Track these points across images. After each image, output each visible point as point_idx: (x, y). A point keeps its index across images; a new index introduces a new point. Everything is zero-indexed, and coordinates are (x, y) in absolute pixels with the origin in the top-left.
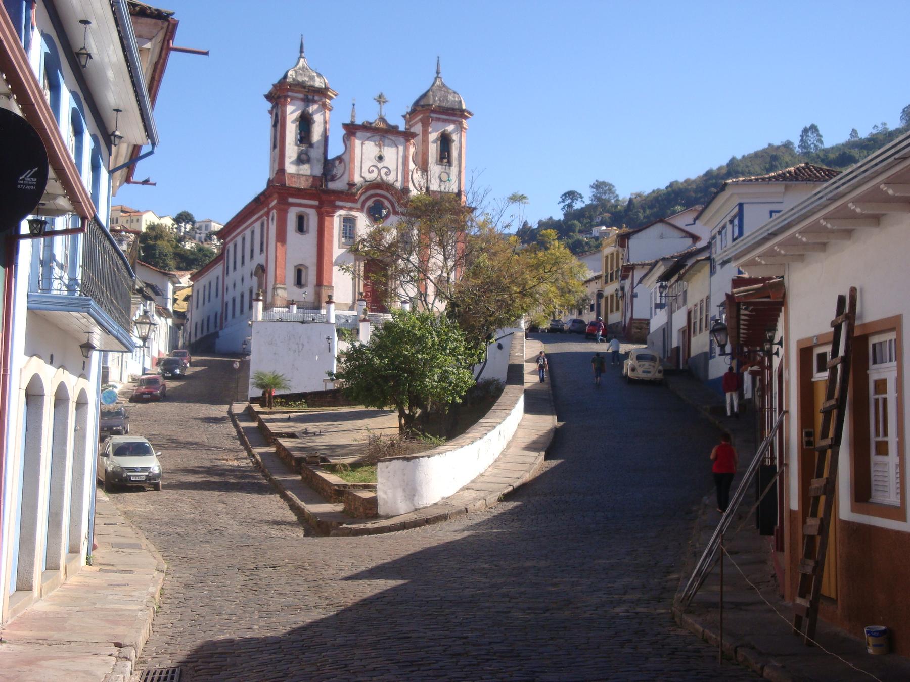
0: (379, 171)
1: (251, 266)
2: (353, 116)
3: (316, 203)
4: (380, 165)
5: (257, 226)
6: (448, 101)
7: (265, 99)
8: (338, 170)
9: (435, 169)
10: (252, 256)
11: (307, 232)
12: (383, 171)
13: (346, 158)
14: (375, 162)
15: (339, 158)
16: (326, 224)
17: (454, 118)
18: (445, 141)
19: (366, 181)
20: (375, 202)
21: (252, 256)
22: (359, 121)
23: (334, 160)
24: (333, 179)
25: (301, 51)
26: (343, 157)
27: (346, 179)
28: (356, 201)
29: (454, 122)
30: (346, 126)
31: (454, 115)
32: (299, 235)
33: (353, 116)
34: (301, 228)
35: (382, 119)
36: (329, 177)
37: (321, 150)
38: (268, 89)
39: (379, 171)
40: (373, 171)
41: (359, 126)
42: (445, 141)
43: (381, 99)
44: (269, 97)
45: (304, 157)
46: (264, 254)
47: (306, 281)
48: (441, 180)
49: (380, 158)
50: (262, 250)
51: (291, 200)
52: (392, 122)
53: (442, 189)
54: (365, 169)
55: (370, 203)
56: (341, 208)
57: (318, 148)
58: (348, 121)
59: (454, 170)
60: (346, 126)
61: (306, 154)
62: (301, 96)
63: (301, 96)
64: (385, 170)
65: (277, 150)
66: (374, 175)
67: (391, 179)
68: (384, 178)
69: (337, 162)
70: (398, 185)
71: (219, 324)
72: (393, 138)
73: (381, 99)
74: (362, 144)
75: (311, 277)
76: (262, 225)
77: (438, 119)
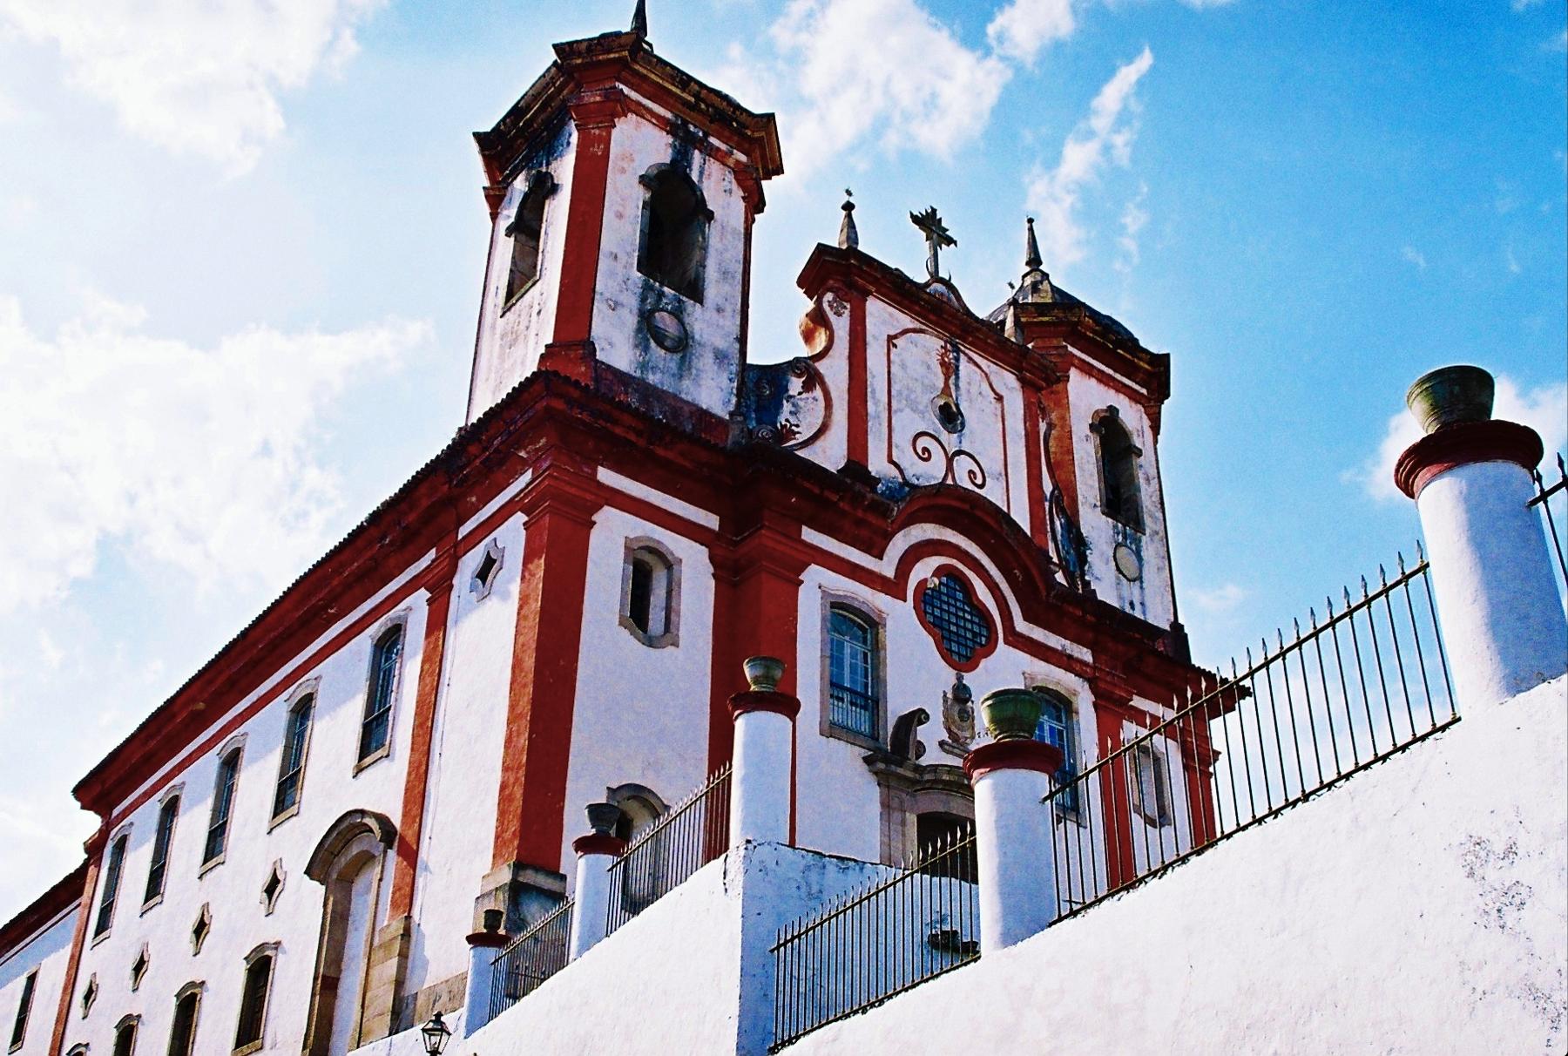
0: (950, 468)
3: (711, 521)
4: (951, 441)
7: (474, 147)
8: (803, 413)
12: (962, 466)
13: (835, 371)
14: (933, 424)
19: (906, 483)
20: (938, 572)
26: (821, 366)
29: (1133, 396)
32: (628, 641)
39: (950, 468)
40: (925, 450)
45: (665, 321)
54: (902, 439)
61: (678, 313)
66: (931, 472)
69: (796, 384)
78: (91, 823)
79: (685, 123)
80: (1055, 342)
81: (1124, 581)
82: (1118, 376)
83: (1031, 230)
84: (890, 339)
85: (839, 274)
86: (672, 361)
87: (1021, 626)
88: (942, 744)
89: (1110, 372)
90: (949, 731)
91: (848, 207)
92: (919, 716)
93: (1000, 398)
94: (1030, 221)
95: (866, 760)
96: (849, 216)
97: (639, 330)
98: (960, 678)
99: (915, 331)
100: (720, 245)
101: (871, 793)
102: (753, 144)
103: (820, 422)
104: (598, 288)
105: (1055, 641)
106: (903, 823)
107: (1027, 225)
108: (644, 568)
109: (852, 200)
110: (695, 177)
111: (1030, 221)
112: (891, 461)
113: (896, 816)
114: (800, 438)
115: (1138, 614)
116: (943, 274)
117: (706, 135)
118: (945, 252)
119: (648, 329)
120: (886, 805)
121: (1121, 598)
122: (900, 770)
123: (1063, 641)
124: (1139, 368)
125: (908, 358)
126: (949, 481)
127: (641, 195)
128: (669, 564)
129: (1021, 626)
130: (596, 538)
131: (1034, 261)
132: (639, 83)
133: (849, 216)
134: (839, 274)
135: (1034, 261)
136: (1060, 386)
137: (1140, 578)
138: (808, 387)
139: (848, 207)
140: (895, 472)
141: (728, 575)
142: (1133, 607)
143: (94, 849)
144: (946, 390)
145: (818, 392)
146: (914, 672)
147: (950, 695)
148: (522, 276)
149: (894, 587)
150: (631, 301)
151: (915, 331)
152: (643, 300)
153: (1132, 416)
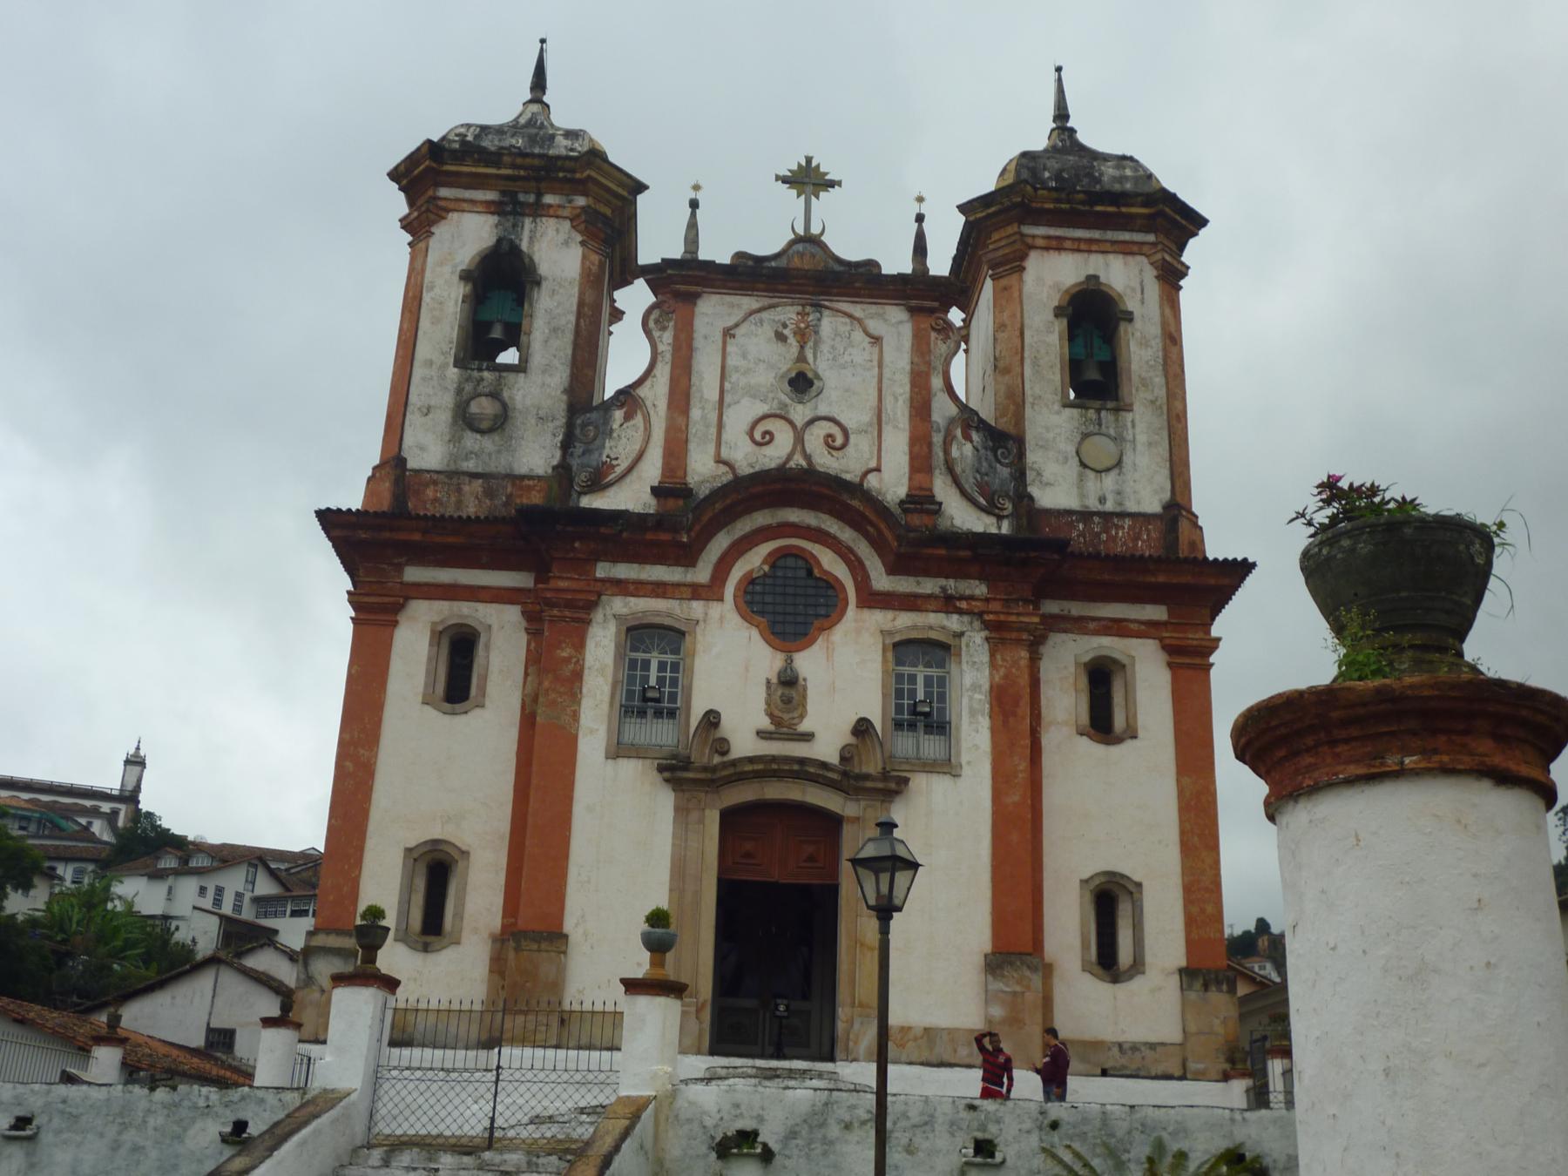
0: (799, 439)
4: (800, 413)
6: (1098, 181)
8: (623, 441)
9: (1052, 426)
15: (628, 397)
17: (1126, 236)
18: (1092, 316)
20: (775, 559)
23: (607, 406)
24: (598, 483)
26: (642, 392)
27: (652, 470)
28: (687, 556)
29: (1126, 249)
31: (1126, 223)
36: (581, 478)
37: (559, 378)
39: (799, 439)
40: (766, 433)
41: (710, 265)
42: (1092, 316)
43: (808, 180)
45: (483, 407)
47: (459, 916)
48: (1083, 465)
49: (802, 383)
51: (414, 574)
52: (847, 246)
53: (1093, 505)
55: (754, 560)
56: (623, 587)
57: (547, 369)
59: (1142, 423)
61: (495, 395)
62: (491, 195)
63: (491, 195)
64: (822, 429)
66: (777, 453)
67: (848, 465)
68: (825, 461)
69: (618, 415)
70: (893, 484)
72: (857, 310)
74: (728, 333)
75: (480, 898)
77: (1057, 245)
79: (513, 195)
80: (1010, 230)
81: (1091, 475)
82: (1111, 235)
83: (1060, 80)
84: (728, 333)
86: (487, 443)
87: (882, 581)
88: (761, 734)
89: (1096, 234)
90: (771, 715)
91: (694, 204)
92: (712, 720)
93: (876, 340)
94: (1059, 69)
95: (661, 769)
96: (693, 215)
97: (455, 422)
98: (789, 661)
99: (759, 310)
101: (666, 800)
103: (637, 447)
104: (413, 398)
105: (929, 586)
106: (701, 821)
107: (1053, 75)
109: (700, 196)
110: (524, 246)
111: (1059, 69)
112: (719, 460)
113: (694, 815)
114: (619, 470)
115: (1110, 506)
116: (815, 230)
117: (539, 195)
119: (464, 419)
120: (680, 811)
121: (1082, 496)
122: (691, 775)
123: (942, 582)
124: (1132, 217)
126: (799, 461)
129: (882, 581)
131: (1062, 115)
132: (455, 180)
133: (693, 215)
135: (1062, 115)
136: (1015, 277)
137: (1119, 464)
138: (628, 417)
139: (694, 204)
140: (724, 469)
142: (1102, 500)
144: (801, 358)
145: (638, 420)
146: (729, 667)
147: (774, 680)
149: (709, 592)
150: (448, 400)
151: (759, 310)
152: (459, 391)
153: (1123, 275)
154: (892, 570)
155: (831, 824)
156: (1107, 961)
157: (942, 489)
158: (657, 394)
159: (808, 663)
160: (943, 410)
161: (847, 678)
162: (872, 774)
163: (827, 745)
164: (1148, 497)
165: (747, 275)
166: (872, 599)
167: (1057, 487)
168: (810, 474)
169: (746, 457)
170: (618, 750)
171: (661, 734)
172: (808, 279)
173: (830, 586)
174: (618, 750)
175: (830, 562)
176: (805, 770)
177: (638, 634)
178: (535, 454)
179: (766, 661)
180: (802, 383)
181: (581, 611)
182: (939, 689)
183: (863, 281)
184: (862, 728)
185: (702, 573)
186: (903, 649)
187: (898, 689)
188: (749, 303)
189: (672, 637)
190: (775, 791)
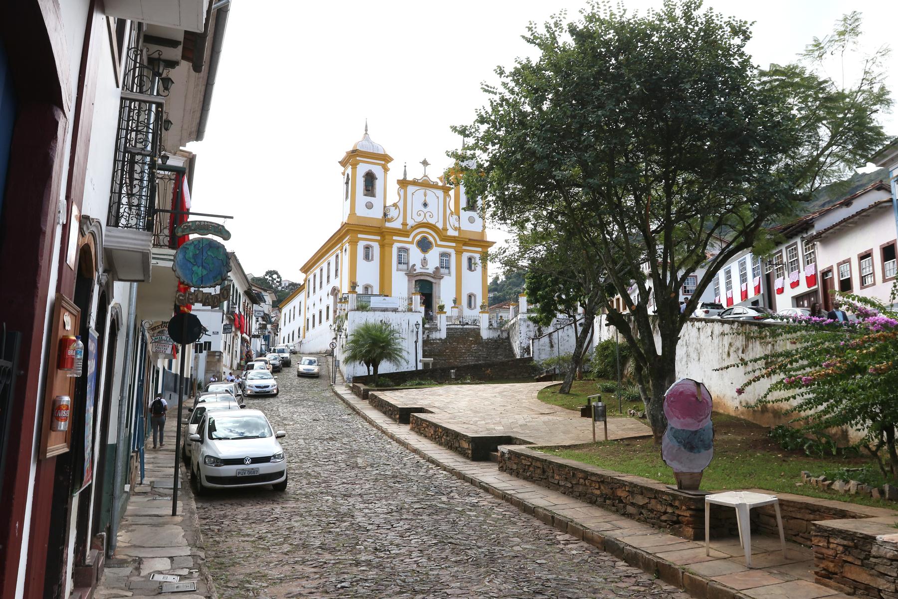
1: (328, 288)
2: (405, 174)
3: (378, 238)
4: (425, 210)
5: (332, 259)
10: (328, 281)
11: (372, 259)
14: (422, 208)
15: (395, 205)
16: (386, 253)
21: (328, 281)
22: (410, 178)
25: (366, 130)
27: (401, 220)
30: (399, 182)
33: (405, 174)
34: (367, 257)
35: (425, 176)
38: (342, 156)
44: (343, 163)
46: (339, 279)
49: (425, 205)
50: (336, 275)
55: (418, 238)
58: (401, 178)
60: (399, 182)
65: (349, 200)
71: (301, 335)
73: (425, 163)
76: (337, 256)
78: (304, 275)
85: (404, 183)
87: (439, 243)
92: (414, 265)
100: (379, 184)
101: (406, 278)
102: (385, 159)
108: (367, 248)
118: (428, 167)
120: (409, 280)
125: (416, 195)
127: (363, 180)
128: (372, 247)
129: (439, 243)
130: (359, 247)
134: (404, 183)
141: (382, 246)
143: (305, 281)
146: (415, 256)
148: (347, 198)
149: (412, 243)
154: (441, 240)
155: (431, 283)
156: (470, 305)
157: (448, 227)
158: (401, 205)
159: (427, 255)
160: (448, 212)
161: (433, 258)
162: (437, 275)
163: (431, 269)
164: (480, 230)
165: (415, 183)
166: (438, 246)
167: (466, 226)
168: (428, 223)
169: (419, 219)
170: (398, 270)
171: (404, 267)
172: (425, 184)
173: (430, 243)
174: (398, 270)
175: (431, 239)
176: (428, 275)
177: (401, 250)
178: (379, 215)
179: (421, 255)
180: (425, 205)
181: (391, 245)
182: (448, 262)
183: (435, 186)
184: (437, 268)
185: (410, 239)
186: (443, 255)
187: (441, 261)
188: (418, 188)
189: (406, 250)
190: (422, 278)
